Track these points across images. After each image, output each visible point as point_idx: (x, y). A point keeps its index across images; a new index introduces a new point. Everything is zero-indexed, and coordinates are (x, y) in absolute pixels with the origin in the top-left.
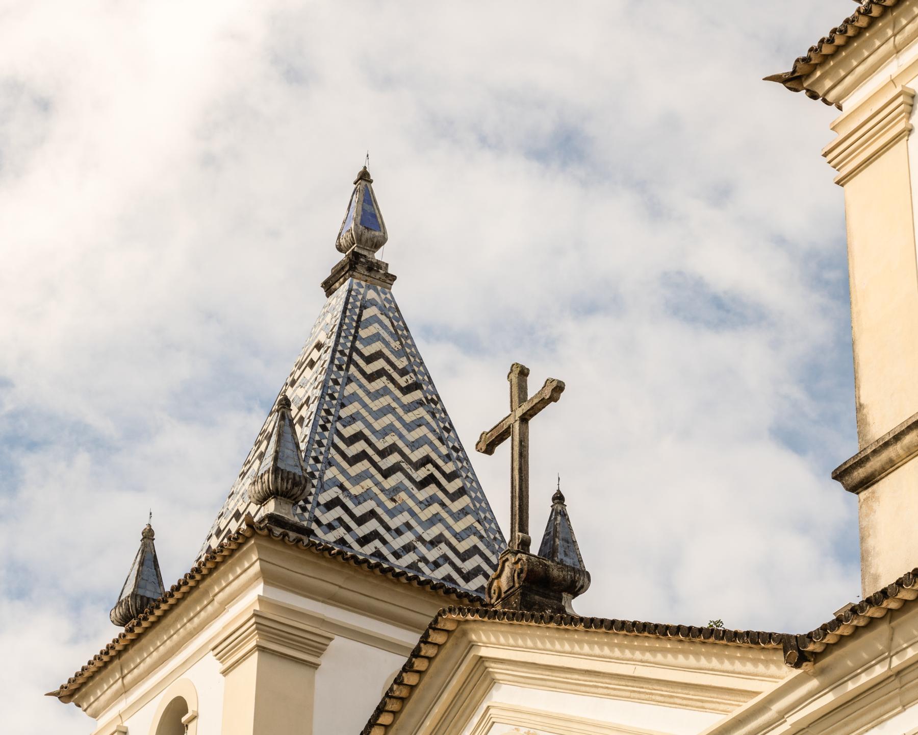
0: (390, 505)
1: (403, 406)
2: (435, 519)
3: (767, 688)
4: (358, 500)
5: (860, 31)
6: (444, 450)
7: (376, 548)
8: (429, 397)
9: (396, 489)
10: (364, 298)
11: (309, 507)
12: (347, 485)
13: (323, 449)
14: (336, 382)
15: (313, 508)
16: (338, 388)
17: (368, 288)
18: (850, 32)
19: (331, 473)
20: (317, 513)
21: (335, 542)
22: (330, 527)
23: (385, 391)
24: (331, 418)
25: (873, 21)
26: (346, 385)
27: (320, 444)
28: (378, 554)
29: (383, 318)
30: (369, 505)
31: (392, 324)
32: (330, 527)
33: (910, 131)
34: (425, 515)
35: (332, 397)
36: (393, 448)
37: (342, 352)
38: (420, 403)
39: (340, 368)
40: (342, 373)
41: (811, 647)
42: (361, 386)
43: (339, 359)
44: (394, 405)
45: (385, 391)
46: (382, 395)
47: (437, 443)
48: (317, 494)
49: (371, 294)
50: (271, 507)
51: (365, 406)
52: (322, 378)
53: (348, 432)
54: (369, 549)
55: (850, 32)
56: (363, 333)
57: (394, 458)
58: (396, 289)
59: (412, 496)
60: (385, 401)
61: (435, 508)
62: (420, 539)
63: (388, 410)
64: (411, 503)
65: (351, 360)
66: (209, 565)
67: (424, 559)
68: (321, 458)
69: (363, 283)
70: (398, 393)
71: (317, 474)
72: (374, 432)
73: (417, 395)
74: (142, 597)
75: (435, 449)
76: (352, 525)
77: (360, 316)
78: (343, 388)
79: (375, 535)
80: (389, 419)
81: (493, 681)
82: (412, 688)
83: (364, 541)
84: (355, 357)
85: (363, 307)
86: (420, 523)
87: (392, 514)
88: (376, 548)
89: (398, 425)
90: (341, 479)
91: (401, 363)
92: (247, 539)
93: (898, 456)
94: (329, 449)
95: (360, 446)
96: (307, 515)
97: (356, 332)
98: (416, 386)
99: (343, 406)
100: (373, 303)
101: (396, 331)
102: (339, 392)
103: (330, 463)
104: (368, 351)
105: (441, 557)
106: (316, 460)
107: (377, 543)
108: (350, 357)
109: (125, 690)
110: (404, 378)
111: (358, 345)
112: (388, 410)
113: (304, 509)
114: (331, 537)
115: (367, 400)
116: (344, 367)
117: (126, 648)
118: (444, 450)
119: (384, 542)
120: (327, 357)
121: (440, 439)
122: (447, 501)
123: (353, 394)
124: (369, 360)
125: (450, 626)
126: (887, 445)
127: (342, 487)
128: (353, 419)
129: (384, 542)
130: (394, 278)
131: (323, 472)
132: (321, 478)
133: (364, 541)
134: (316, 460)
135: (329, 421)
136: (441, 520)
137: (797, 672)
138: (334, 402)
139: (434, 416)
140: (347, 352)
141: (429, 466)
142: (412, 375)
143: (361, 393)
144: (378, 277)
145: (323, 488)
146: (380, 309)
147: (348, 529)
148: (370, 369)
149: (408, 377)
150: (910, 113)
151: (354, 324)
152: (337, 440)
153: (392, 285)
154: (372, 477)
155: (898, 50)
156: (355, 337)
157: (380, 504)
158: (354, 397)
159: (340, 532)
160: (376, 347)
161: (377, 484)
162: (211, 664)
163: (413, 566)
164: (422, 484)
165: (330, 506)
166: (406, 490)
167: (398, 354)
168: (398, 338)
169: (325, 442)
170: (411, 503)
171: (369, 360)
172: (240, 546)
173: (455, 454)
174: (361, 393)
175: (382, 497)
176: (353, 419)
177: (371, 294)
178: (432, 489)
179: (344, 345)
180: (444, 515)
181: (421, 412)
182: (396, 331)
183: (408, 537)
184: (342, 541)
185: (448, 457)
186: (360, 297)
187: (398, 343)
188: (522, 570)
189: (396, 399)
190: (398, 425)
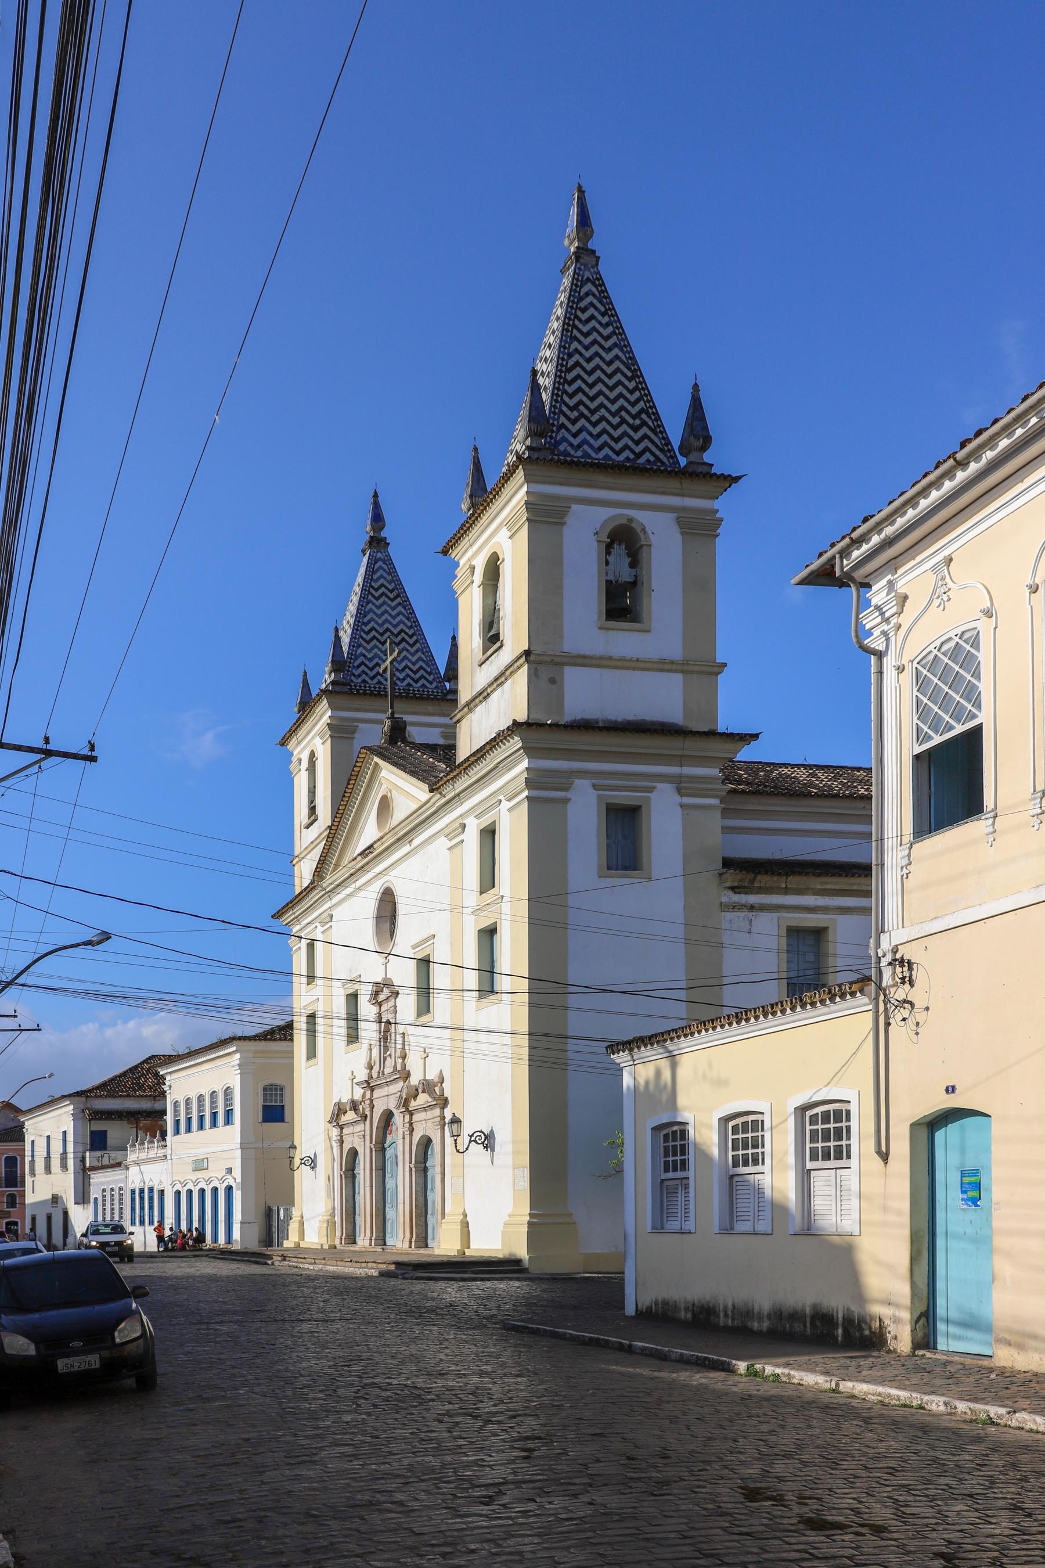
6: (409, 624)
17: (378, 552)
20: (354, 671)
32: (359, 676)
38: (399, 604)
39: (364, 598)
47: (406, 621)
49: (379, 555)
56: (375, 577)
58: (390, 549)
78: (365, 608)
84: (372, 590)
85: (376, 563)
90: (364, 652)
98: (398, 596)
99: (365, 616)
100: (380, 559)
103: (359, 646)
106: (354, 646)
108: (369, 591)
111: (373, 584)
118: (409, 624)
139: (405, 608)
148: (377, 594)
158: (371, 610)
165: (359, 666)
167: (390, 582)
168: (389, 574)
176: (369, 621)
177: (379, 555)
181: (400, 608)
185: (410, 627)
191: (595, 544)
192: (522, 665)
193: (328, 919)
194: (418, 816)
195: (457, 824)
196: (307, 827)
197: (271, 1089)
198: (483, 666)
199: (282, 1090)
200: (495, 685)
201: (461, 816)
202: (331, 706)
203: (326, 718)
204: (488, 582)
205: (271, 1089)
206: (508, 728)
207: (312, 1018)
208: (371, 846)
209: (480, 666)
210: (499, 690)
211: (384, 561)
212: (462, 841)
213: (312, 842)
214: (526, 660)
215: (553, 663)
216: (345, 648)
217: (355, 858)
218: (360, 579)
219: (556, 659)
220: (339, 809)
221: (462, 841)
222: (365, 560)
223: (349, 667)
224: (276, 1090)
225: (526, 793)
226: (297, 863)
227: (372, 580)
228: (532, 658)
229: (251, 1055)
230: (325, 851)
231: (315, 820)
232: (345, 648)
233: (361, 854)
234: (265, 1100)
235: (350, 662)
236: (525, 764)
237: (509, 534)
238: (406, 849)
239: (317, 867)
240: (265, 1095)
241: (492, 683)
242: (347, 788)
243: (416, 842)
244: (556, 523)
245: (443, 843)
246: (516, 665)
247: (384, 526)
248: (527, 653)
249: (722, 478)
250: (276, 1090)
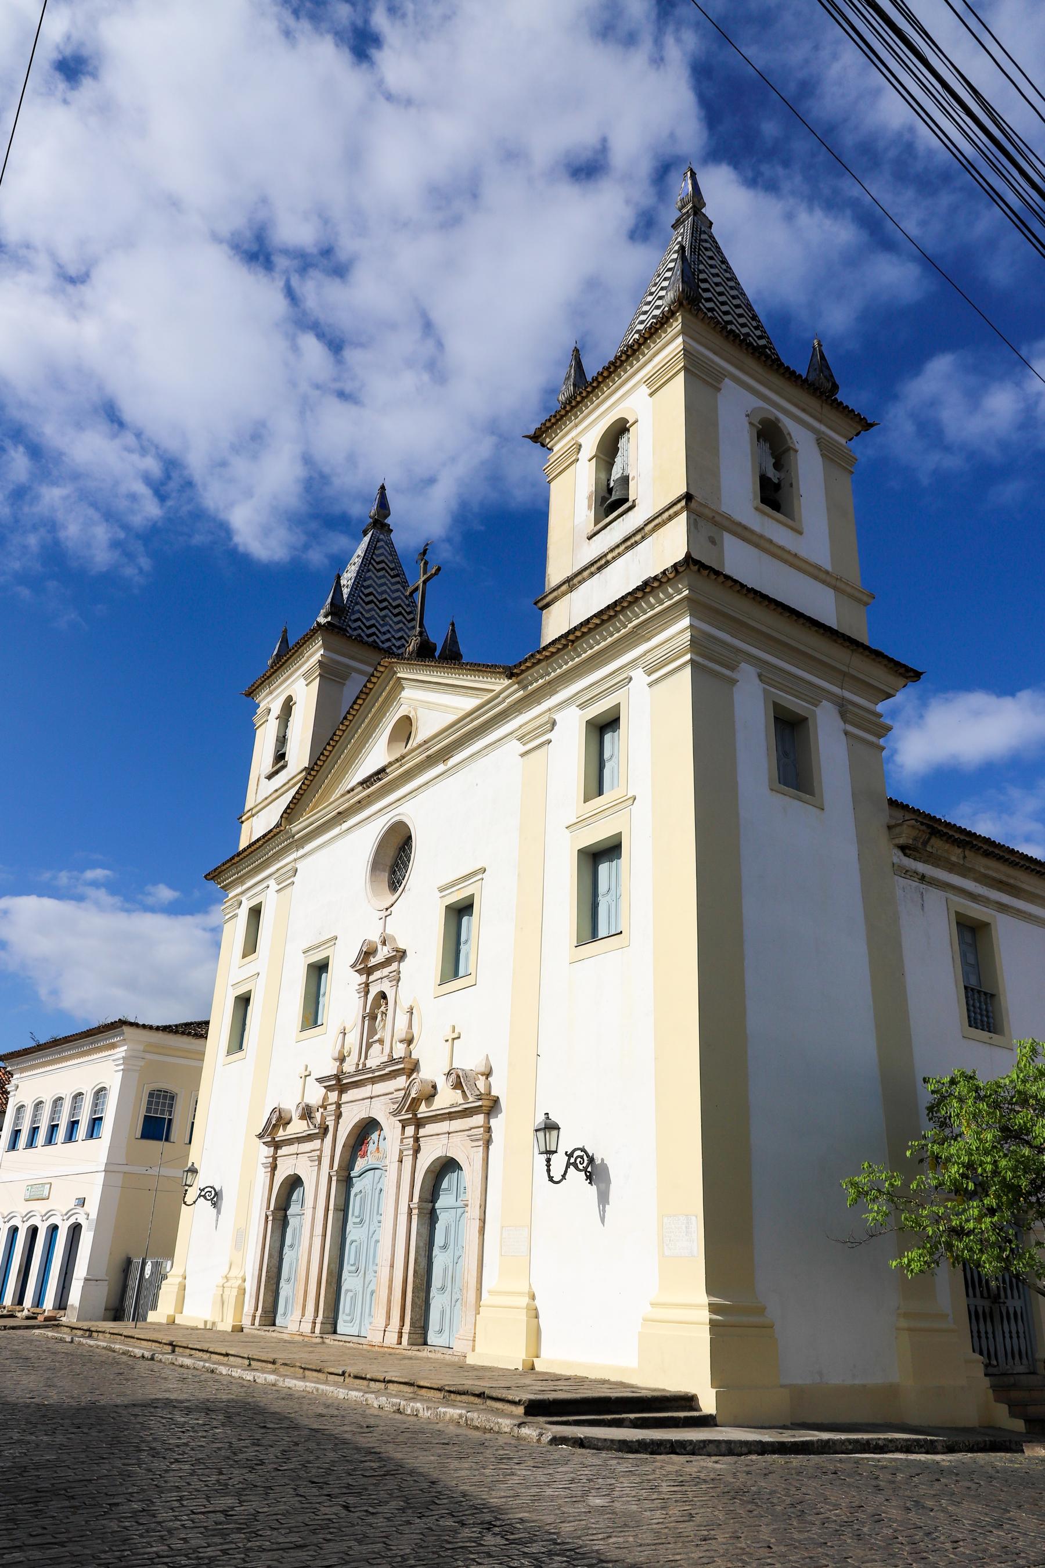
0: (382, 622)
1: (391, 583)
2: (401, 629)
3: (498, 688)
4: (368, 619)
5: (562, 417)
6: (407, 602)
9: (385, 616)
12: (364, 613)
14: (363, 571)
17: (381, 534)
18: (558, 417)
19: (357, 607)
20: (350, 623)
22: (355, 629)
23: (384, 577)
25: (567, 412)
27: (354, 596)
28: (375, 641)
29: (386, 547)
30: (373, 622)
32: (355, 629)
33: (578, 460)
34: (396, 627)
35: (361, 577)
36: (385, 600)
37: (367, 559)
38: (398, 582)
41: (515, 671)
42: (374, 573)
44: (387, 582)
45: (384, 577)
49: (382, 537)
50: (329, 619)
51: (375, 582)
52: (357, 569)
53: (367, 591)
54: (371, 639)
55: (558, 417)
56: (377, 552)
57: (385, 604)
59: (392, 620)
60: (383, 580)
61: (401, 625)
62: (393, 637)
63: (385, 584)
64: (391, 622)
65: (370, 563)
66: (302, 641)
67: (394, 645)
70: (389, 578)
72: (377, 592)
73: (398, 579)
76: (365, 629)
78: (366, 574)
79: (374, 634)
80: (384, 588)
81: (403, 688)
82: (371, 689)
83: (369, 636)
86: (394, 630)
87: (382, 626)
89: (388, 590)
90: (362, 610)
91: (392, 566)
92: (317, 631)
93: (559, 595)
95: (371, 598)
98: (397, 575)
99: (365, 581)
100: (382, 540)
103: (357, 603)
104: (378, 560)
106: (351, 602)
107: (375, 637)
108: (370, 561)
109: (271, 693)
111: (374, 556)
112: (385, 584)
114: (371, 639)
115: (376, 579)
117: (271, 675)
118: (407, 602)
119: (378, 637)
120: (360, 561)
122: (406, 623)
124: (378, 563)
125: (386, 664)
126: (554, 590)
127: (361, 613)
128: (368, 587)
129: (378, 637)
130: (392, 531)
131: (354, 607)
132: (353, 609)
133: (369, 636)
136: (403, 630)
137: (507, 682)
141: (400, 608)
143: (373, 576)
145: (353, 613)
147: (363, 631)
148: (378, 567)
150: (578, 453)
152: (361, 594)
154: (375, 610)
155: (576, 426)
156: (373, 553)
157: (377, 621)
158: (370, 578)
160: (382, 558)
161: (377, 613)
162: (302, 682)
163: (389, 647)
164: (396, 615)
165: (356, 621)
166: (389, 617)
167: (391, 562)
170: (391, 622)
171: (378, 563)
172: (315, 633)
174: (373, 576)
175: (379, 619)
176: (368, 587)
177: (382, 537)
178: (400, 618)
179: (368, 556)
180: (404, 628)
181: (399, 586)
183: (388, 636)
185: (408, 605)
188: (417, 644)
189: (388, 580)
190: (388, 590)
191: (747, 425)
192: (677, 514)
193: (291, 873)
194: (472, 721)
196: (269, 777)
197: (158, 1097)
199: (172, 1098)
200: (622, 548)
201: (550, 710)
202: (325, 646)
203: (317, 656)
204: (602, 456)
205: (158, 1097)
206: (675, 566)
207: (244, 1001)
208: (382, 770)
210: (629, 555)
211: (386, 543)
213: (276, 791)
214: (686, 504)
215: (716, 524)
216: (346, 592)
217: (352, 790)
218: (329, 600)
219: (718, 518)
220: (334, 734)
222: (367, 539)
223: (346, 618)
224: (165, 1097)
225: (688, 657)
226: (248, 819)
227: (373, 553)
228: (693, 505)
229: (141, 1048)
230: (306, 782)
231: (284, 767)
232: (346, 592)
233: (361, 783)
234: (148, 1110)
235: (349, 608)
236: (686, 622)
238: (440, 768)
239: (288, 807)
240: (150, 1103)
241: (618, 546)
242: (352, 707)
243: (451, 762)
244: (712, 386)
246: (666, 515)
247: (389, 514)
248: (688, 497)
249: (857, 419)
250: (165, 1097)
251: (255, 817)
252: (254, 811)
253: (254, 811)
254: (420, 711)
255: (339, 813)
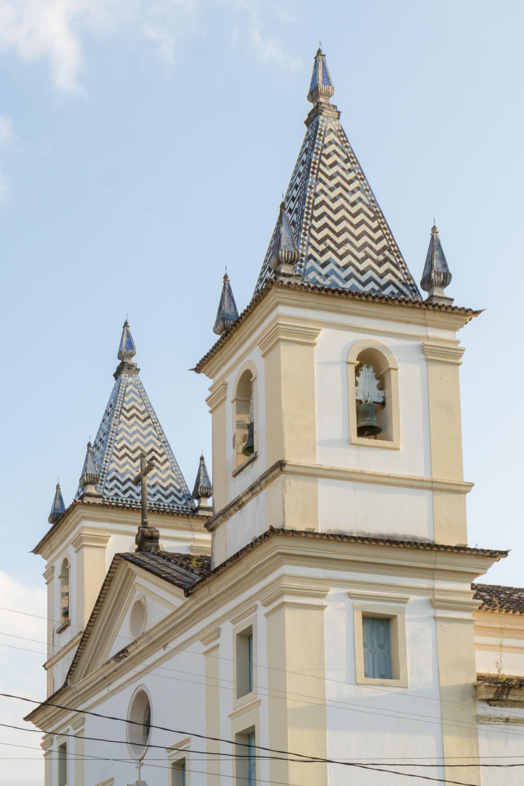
6: (159, 444)
7: (130, 494)
8: (154, 421)
10: (127, 382)
11: (103, 483)
13: (109, 456)
15: (105, 483)
16: (115, 427)
17: (129, 376)
20: (107, 485)
21: (113, 495)
24: (112, 442)
26: (119, 424)
31: (139, 391)
32: (112, 489)
40: (117, 420)
42: (125, 424)
43: (116, 414)
46: (134, 426)
47: (157, 441)
48: (106, 476)
56: (126, 399)
68: (108, 460)
69: (127, 375)
71: (106, 468)
74: (57, 513)
75: (155, 444)
77: (125, 391)
84: (123, 411)
88: (130, 494)
90: (117, 468)
91: (142, 408)
94: (111, 456)
95: (124, 451)
96: (102, 486)
97: (124, 399)
98: (149, 417)
99: (117, 434)
100: (131, 383)
101: (140, 394)
102: (116, 429)
104: (127, 407)
105: (157, 491)
107: (130, 492)
108: (121, 412)
110: (143, 415)
111: (124, 405)
113: (101, 484)
116: (118, 417)
117: (49, 538)
118: (159, 444)
121: (158, 439)
123: (122, 428)
130: (139, 370)
134: (106, 462)
135: (111, 443)
138: (114, 434)
139: (155, 429)
140: (119, 409)
142: (147, 413)
144: (133, 371)
146: (134, 385)
148: (128, 415)
149: (145, 414)
151: (123, 396)
153: (138, 373)
156: (123, 402)
159: (116, 490)
165: (111, 480)
167: (141, 405)
168: (140, 397)
169: (110, 453)
173: (164, 444)
176: (121, 439)
177: (130, 379)
181: (151, 429)
182: (140, 394)
184: (116, 494)
186: (125, 382)
187: (141, 399)
194: (174, 621)
195: (213, 629)
198: (238, 477)
209: (235, 476)
212: (218, 646)
213: (65, 647)
221: (218, 646)
223: (102, 480)
237: (262, 353)
238: (161, 653)
245: (198, 647)
251: (55, 666)
252: (53, 661)
253: (53, 661)
254: (147, 598)
255: (105, 678)
